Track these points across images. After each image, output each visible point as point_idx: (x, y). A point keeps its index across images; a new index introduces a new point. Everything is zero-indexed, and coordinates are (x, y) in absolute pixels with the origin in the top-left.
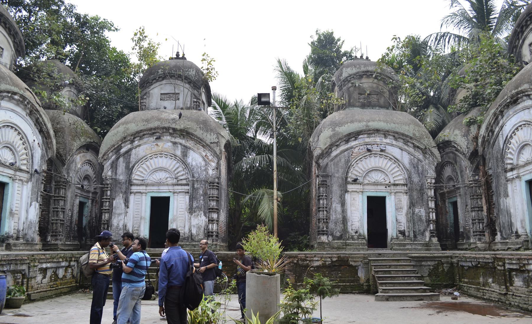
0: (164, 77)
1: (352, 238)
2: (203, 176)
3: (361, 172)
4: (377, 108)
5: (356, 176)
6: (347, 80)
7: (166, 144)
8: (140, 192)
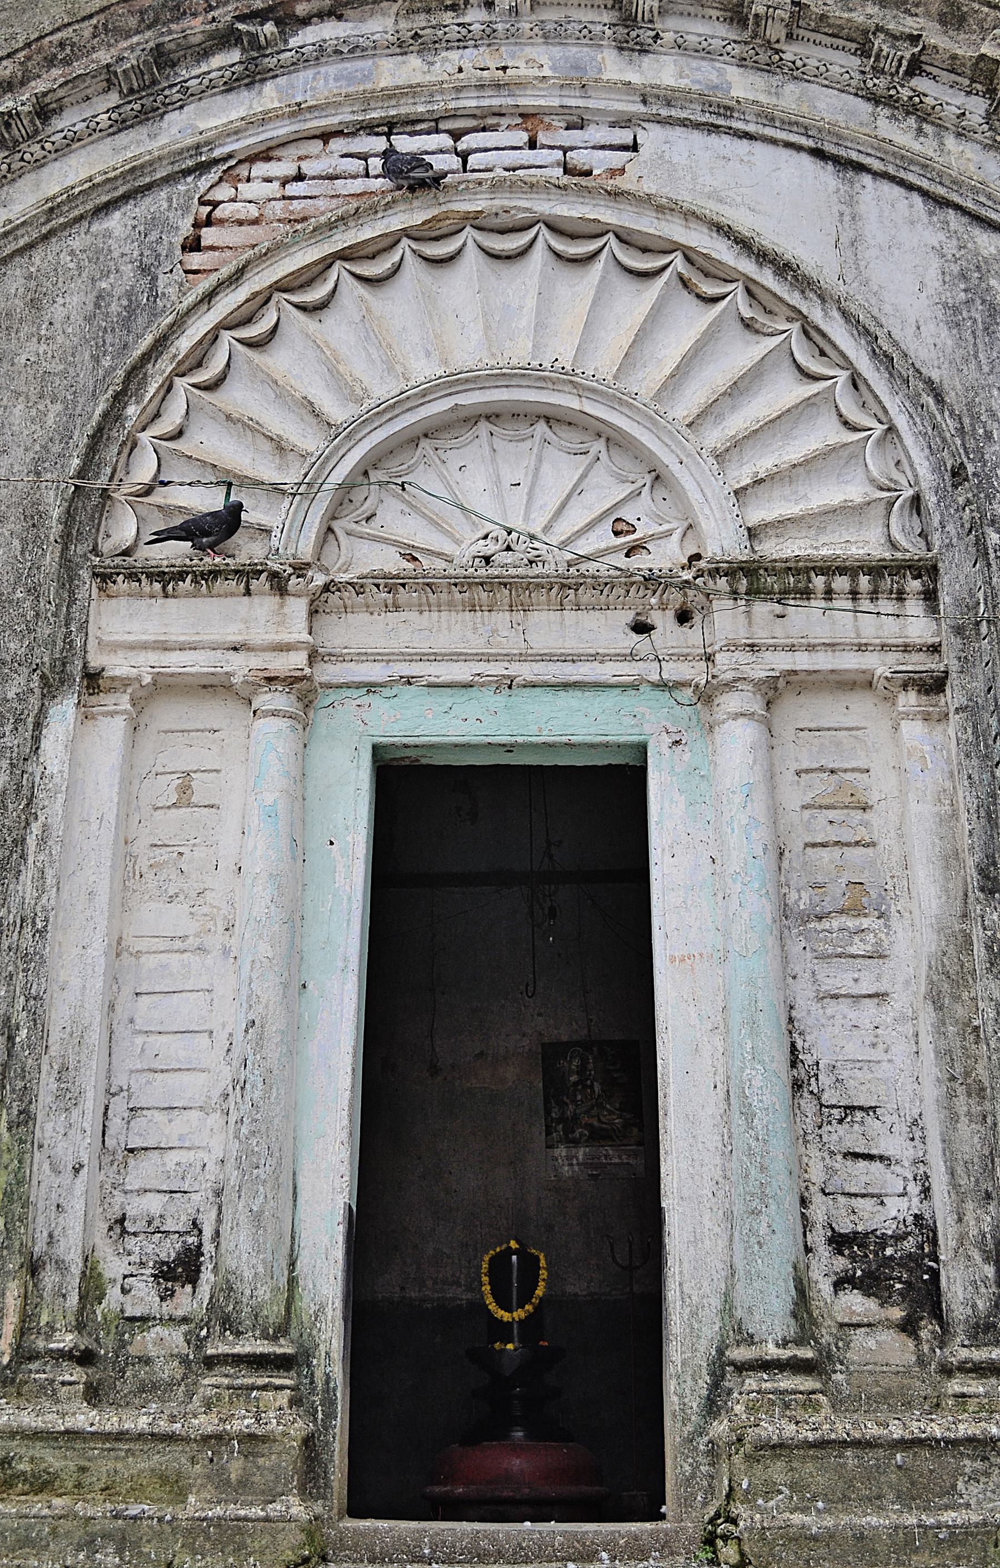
3: (309, 440)
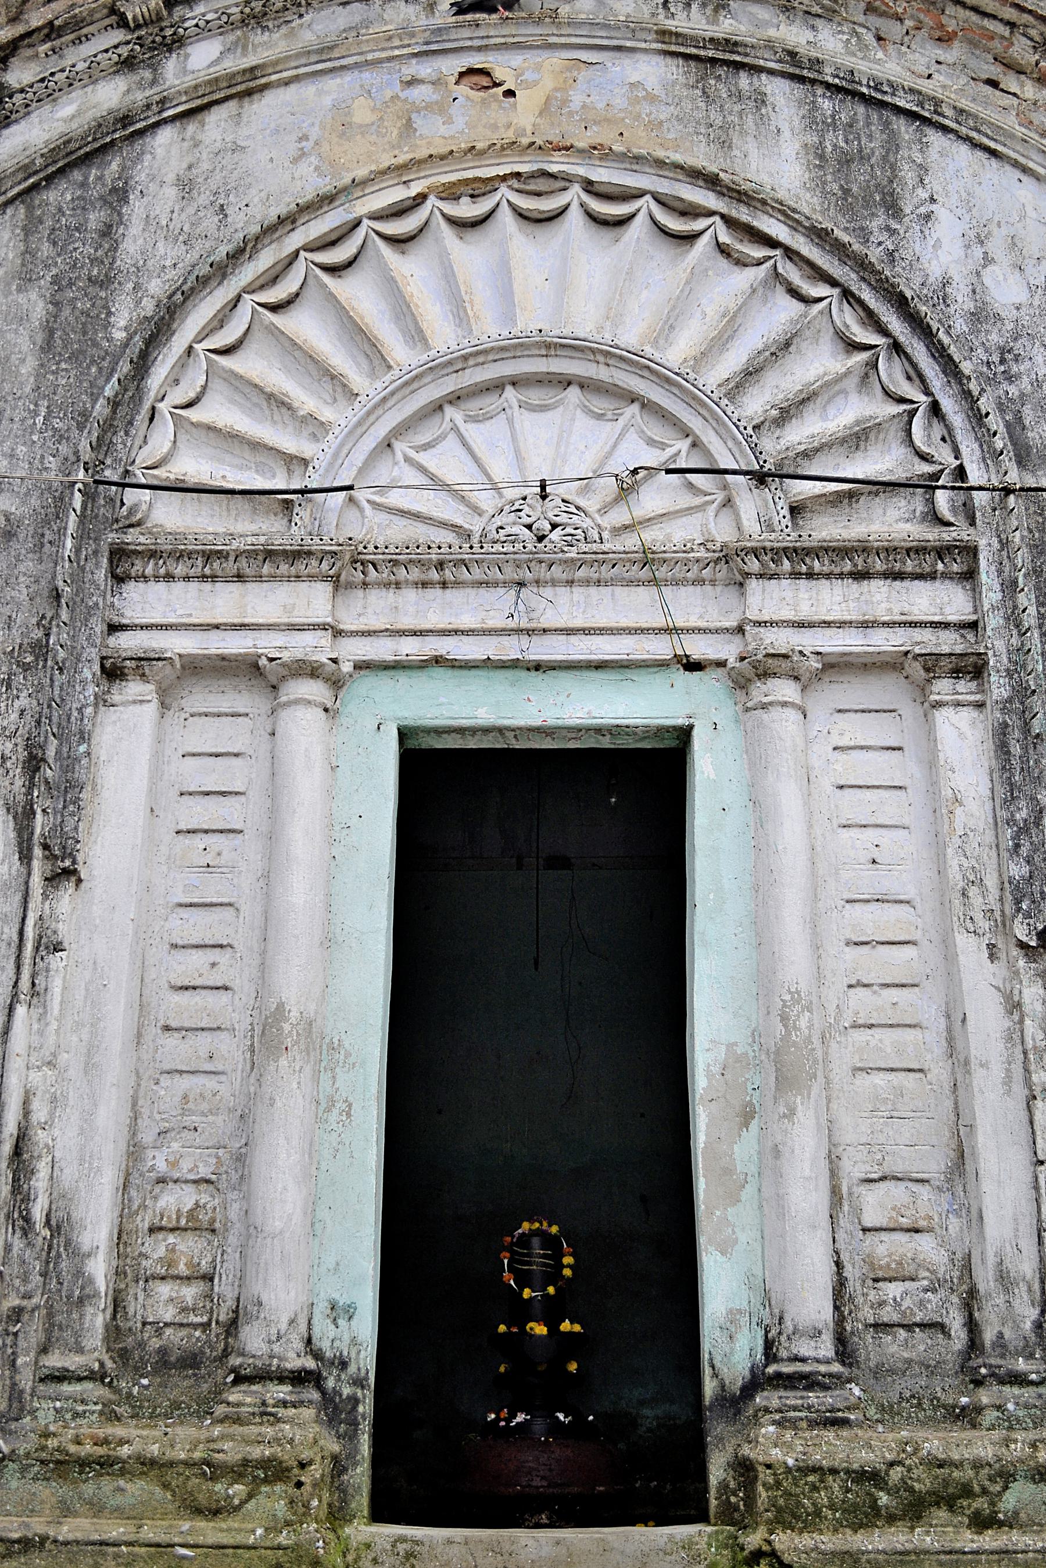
8: (250, 670)
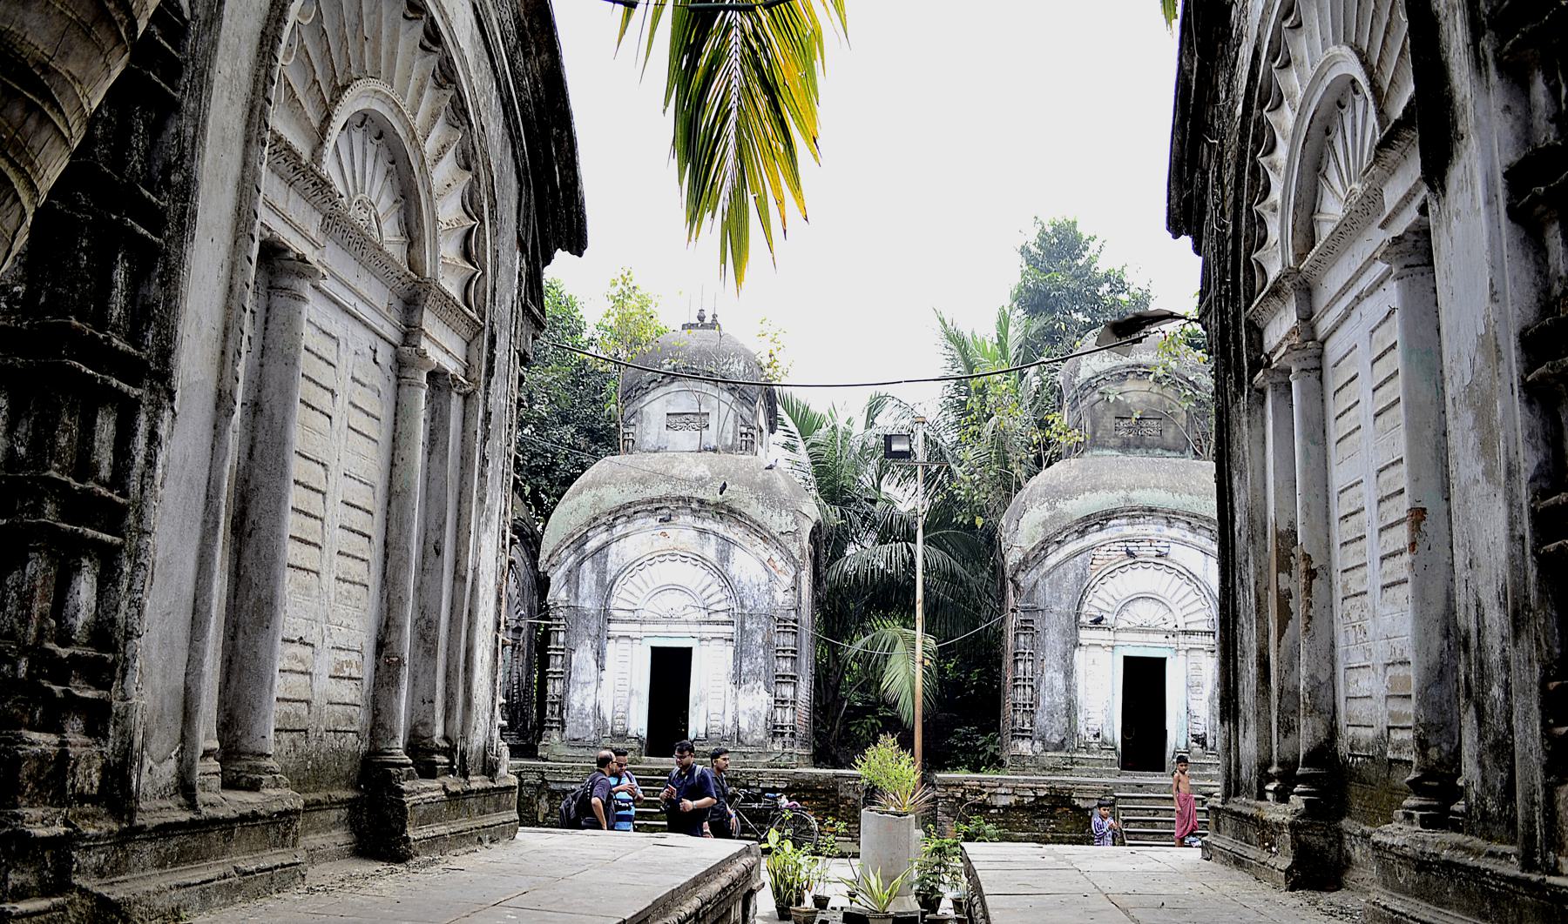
0: (673, 376)
1: (1087, 748)
2: (763, 607)
3: (1112, 602)
4: (1159, 451)
5: (1101, 610)
6: (1090, 386)
7: (683, 532)
